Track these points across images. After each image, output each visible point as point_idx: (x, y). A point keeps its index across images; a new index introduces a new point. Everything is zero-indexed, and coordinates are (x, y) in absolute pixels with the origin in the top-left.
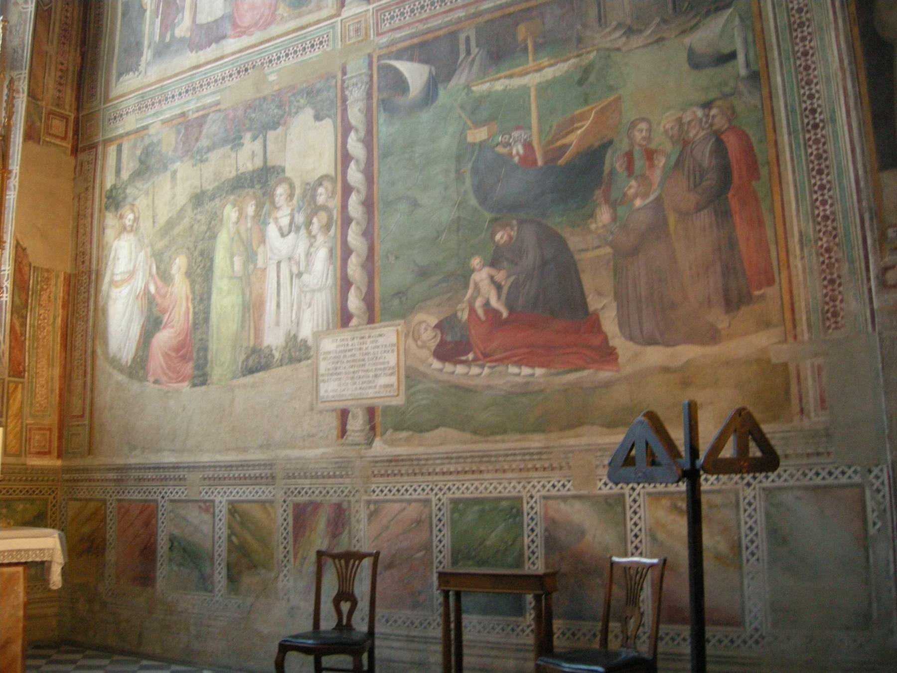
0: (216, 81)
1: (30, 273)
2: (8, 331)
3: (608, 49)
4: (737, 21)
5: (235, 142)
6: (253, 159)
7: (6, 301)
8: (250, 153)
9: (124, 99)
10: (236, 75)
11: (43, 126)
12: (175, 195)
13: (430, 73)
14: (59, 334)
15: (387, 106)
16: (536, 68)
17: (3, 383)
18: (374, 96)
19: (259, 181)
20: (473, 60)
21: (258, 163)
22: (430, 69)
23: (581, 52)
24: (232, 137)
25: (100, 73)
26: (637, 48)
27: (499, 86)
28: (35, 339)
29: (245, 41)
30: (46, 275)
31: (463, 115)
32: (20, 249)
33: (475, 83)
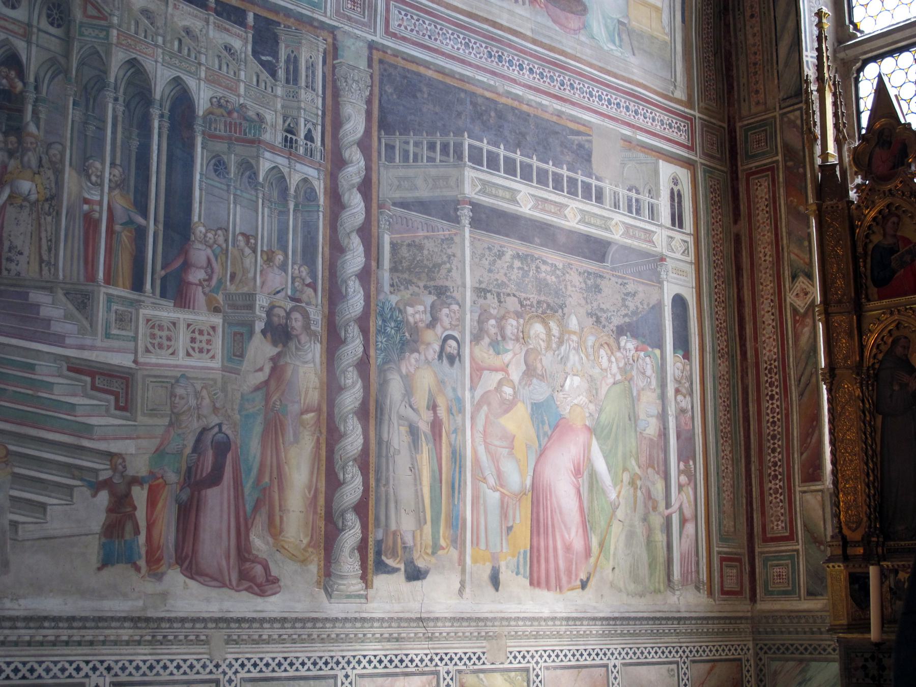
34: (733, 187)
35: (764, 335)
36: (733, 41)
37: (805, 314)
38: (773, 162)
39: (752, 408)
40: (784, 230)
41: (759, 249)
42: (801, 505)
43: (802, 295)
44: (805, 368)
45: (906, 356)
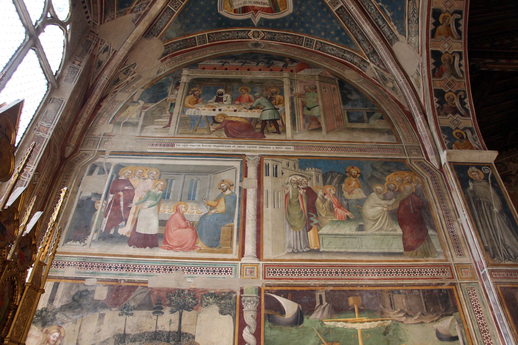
0: (146, 269)
3: (397, 321)
4: (456, 323)
5: (158, 310)
6: (170, 325)
8: (169, 320)
10: (163, 270)
12: (100, 330)
13: (299, 308)
15: (269, 318)
16: (360, 321)
18: (262, 311)
19: (174, 340)
20: (324, 308)
21: (174, 328)
22: (299, 306)
23: (383, 319)
24: (155, 306)
26: (412, 324)
27: (340, 325)
29: (171, 253)
31: (319, 336)
33: (326, 320)
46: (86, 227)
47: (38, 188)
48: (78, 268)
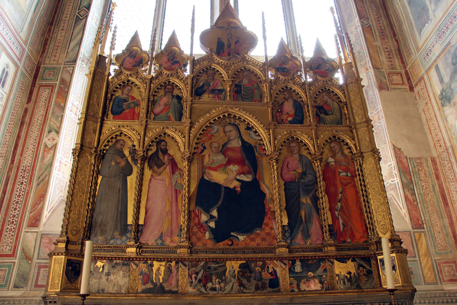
1: (408, 162)
2: (404, 200)
7: (398, 182)
9: (428, 41)
11: (387, 81)
14: (440, 196)
17: (410, 234)
25: (409, 42)
28: (424, 202)
30: (419, 161)
32: (397, 149)
34: (31, 89)
35: (26, 154)
36: (51, 35)
37: (51, 148)
38: (54, 84)
39: (9, 187)
40: (51, 111)
41: (36, 117)
42: (24, 238)
43: (51, 140)
44: (44, 172)
45: (122, 149)
46: (423, 9)
47: (375, 26)
48: (440, 40)
